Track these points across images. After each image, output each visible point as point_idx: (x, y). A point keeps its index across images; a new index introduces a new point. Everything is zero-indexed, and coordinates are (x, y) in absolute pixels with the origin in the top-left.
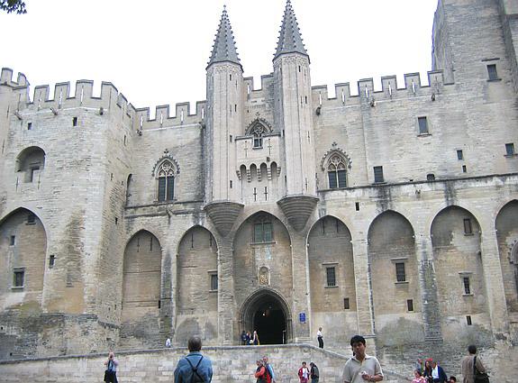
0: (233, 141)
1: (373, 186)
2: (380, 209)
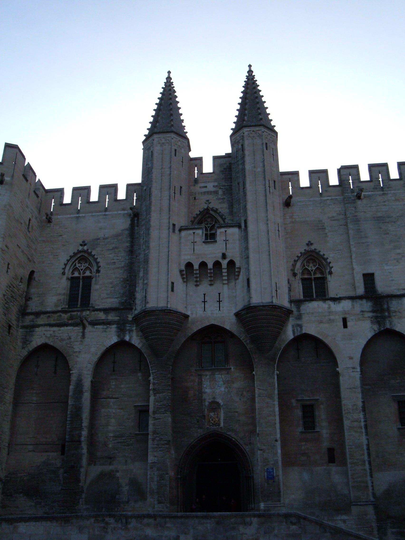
0: (177, 231)
1: (360, 298)
2: (376, 327)
